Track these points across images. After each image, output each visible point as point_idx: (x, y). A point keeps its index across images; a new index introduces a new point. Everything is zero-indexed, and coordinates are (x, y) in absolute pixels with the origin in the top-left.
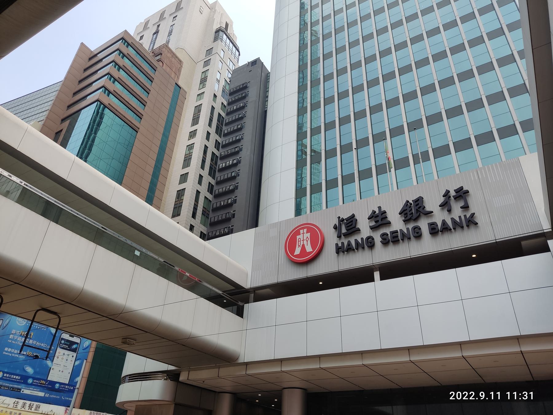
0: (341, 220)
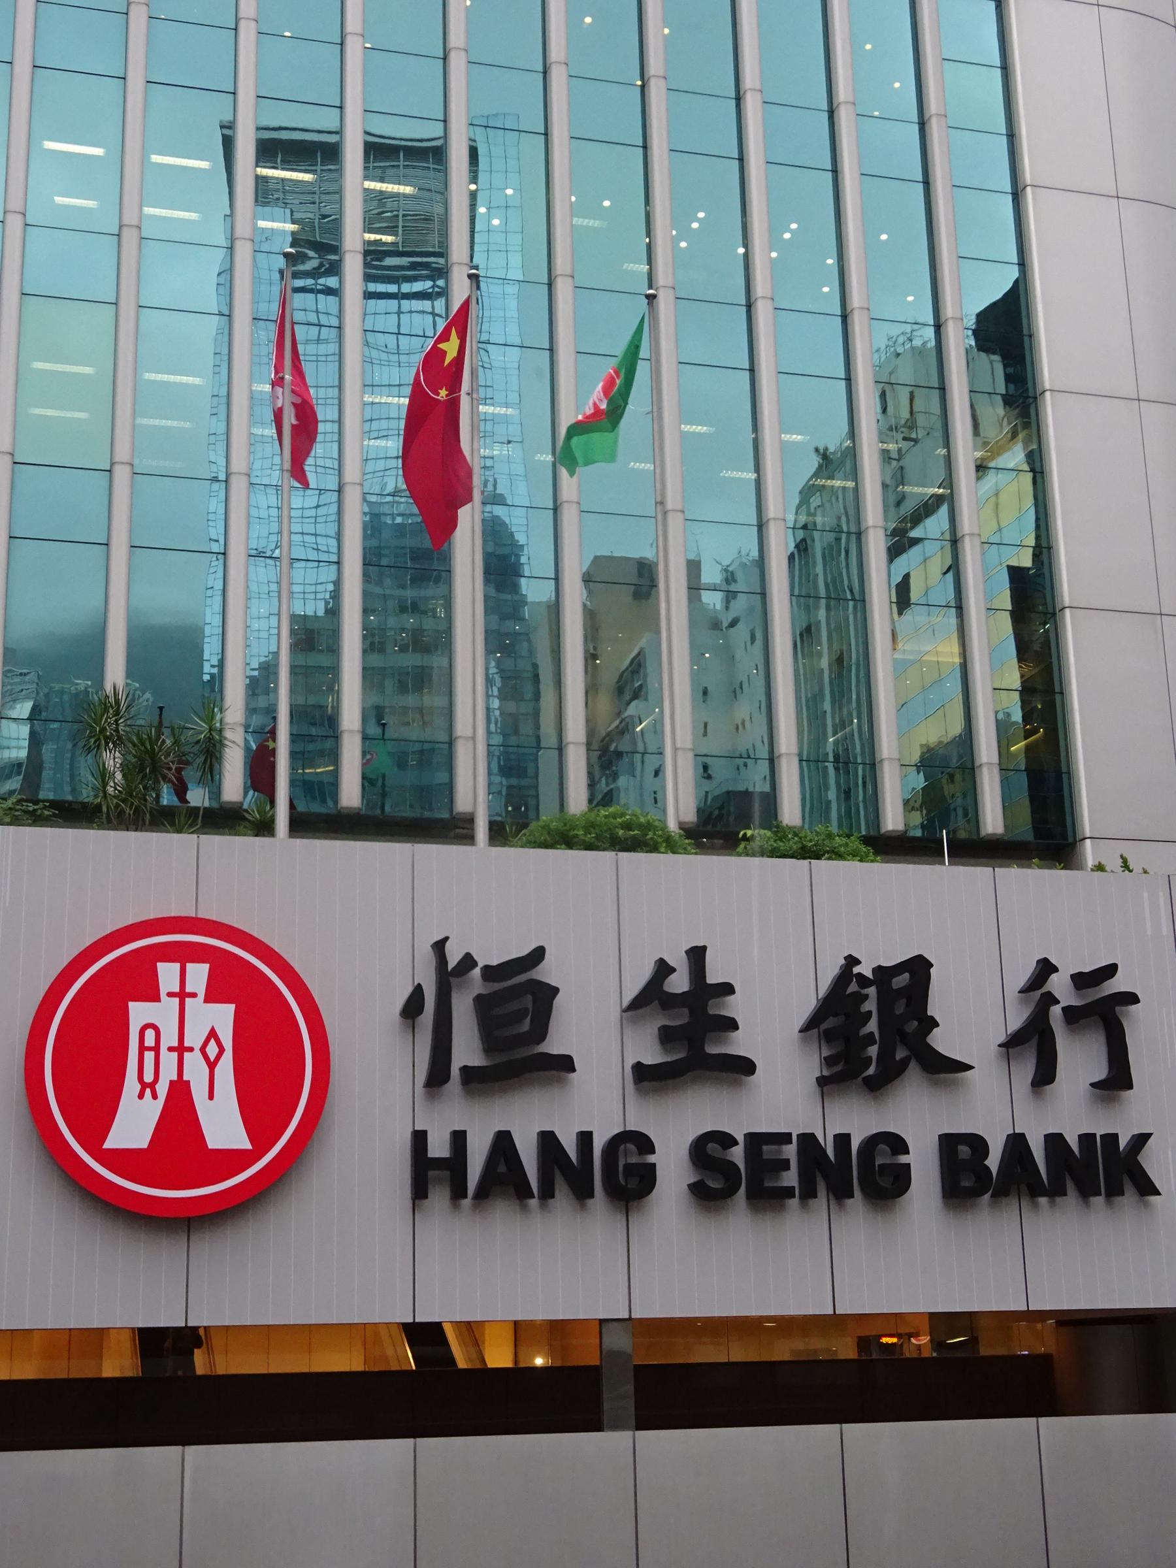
0: (450, 973)
